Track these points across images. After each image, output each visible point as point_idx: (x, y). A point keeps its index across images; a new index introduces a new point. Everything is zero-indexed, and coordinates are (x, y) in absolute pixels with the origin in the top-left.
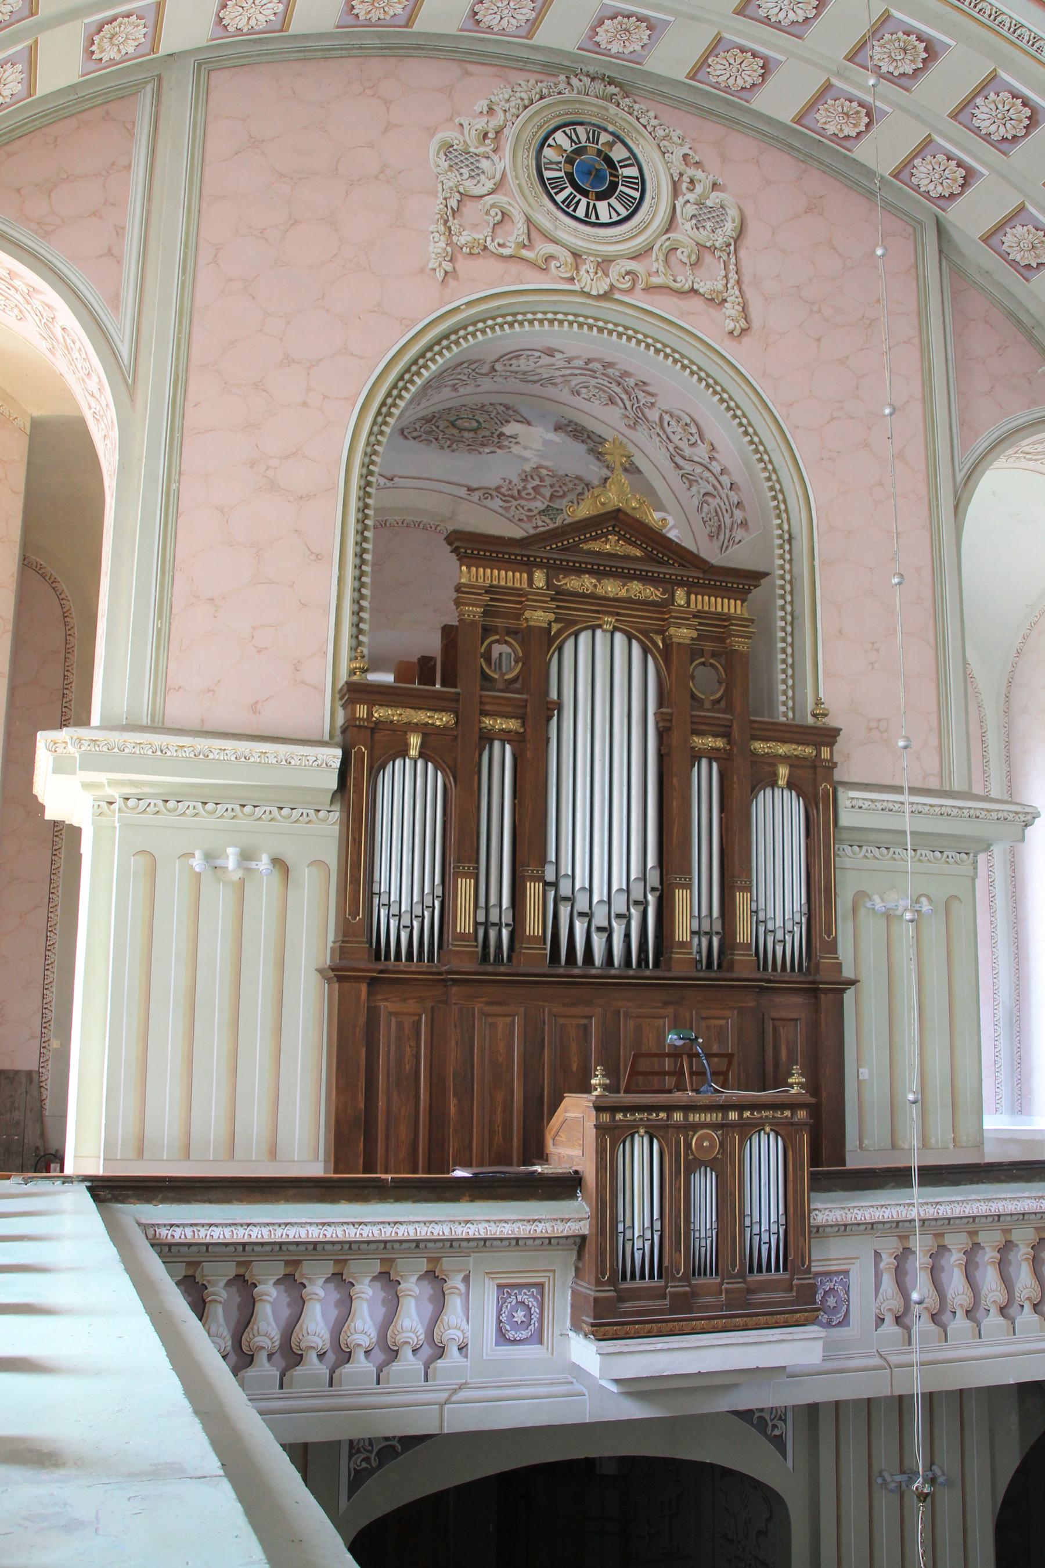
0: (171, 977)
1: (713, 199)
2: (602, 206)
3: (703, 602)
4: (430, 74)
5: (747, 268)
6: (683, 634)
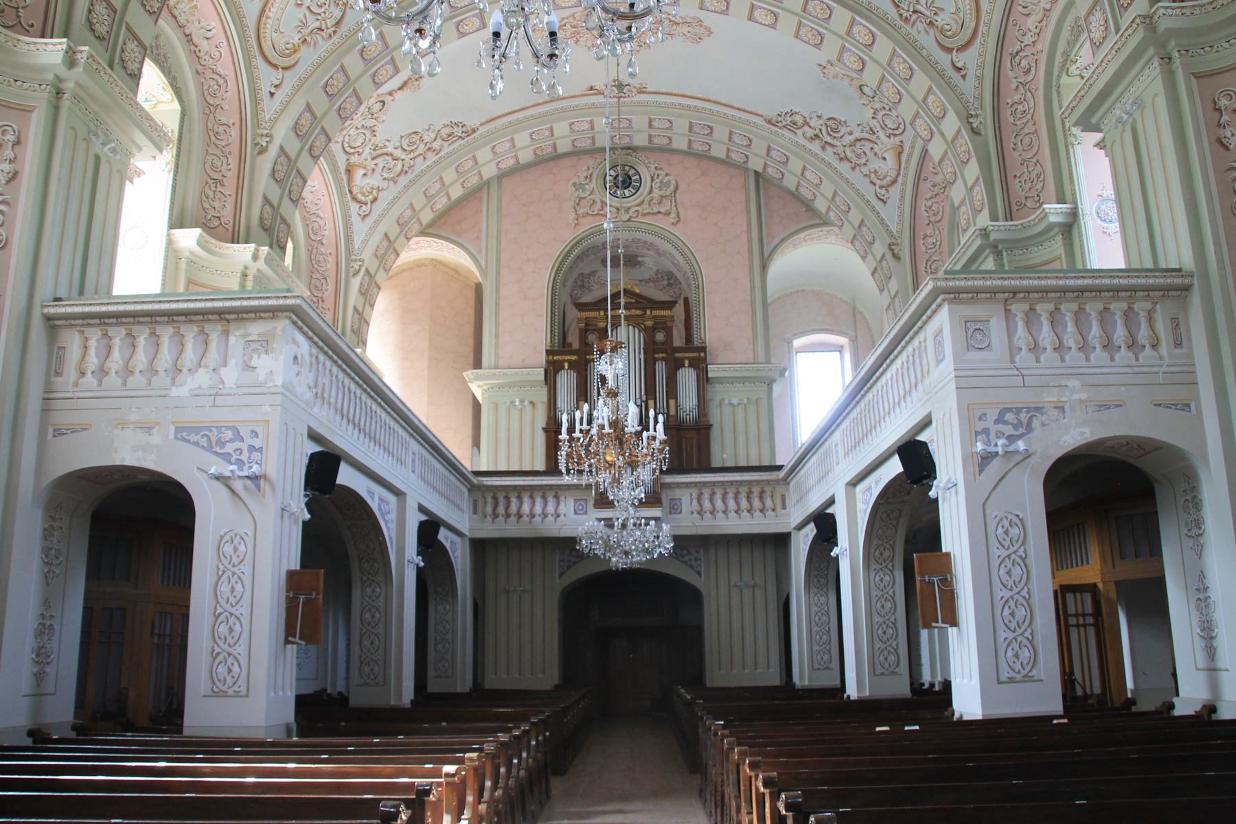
0: (503, 435)
1: (666, 179)
2: (626, 191)
3: (656, 313)
4: (567, 162)
5: (679, 201)
6: (650, 323)
